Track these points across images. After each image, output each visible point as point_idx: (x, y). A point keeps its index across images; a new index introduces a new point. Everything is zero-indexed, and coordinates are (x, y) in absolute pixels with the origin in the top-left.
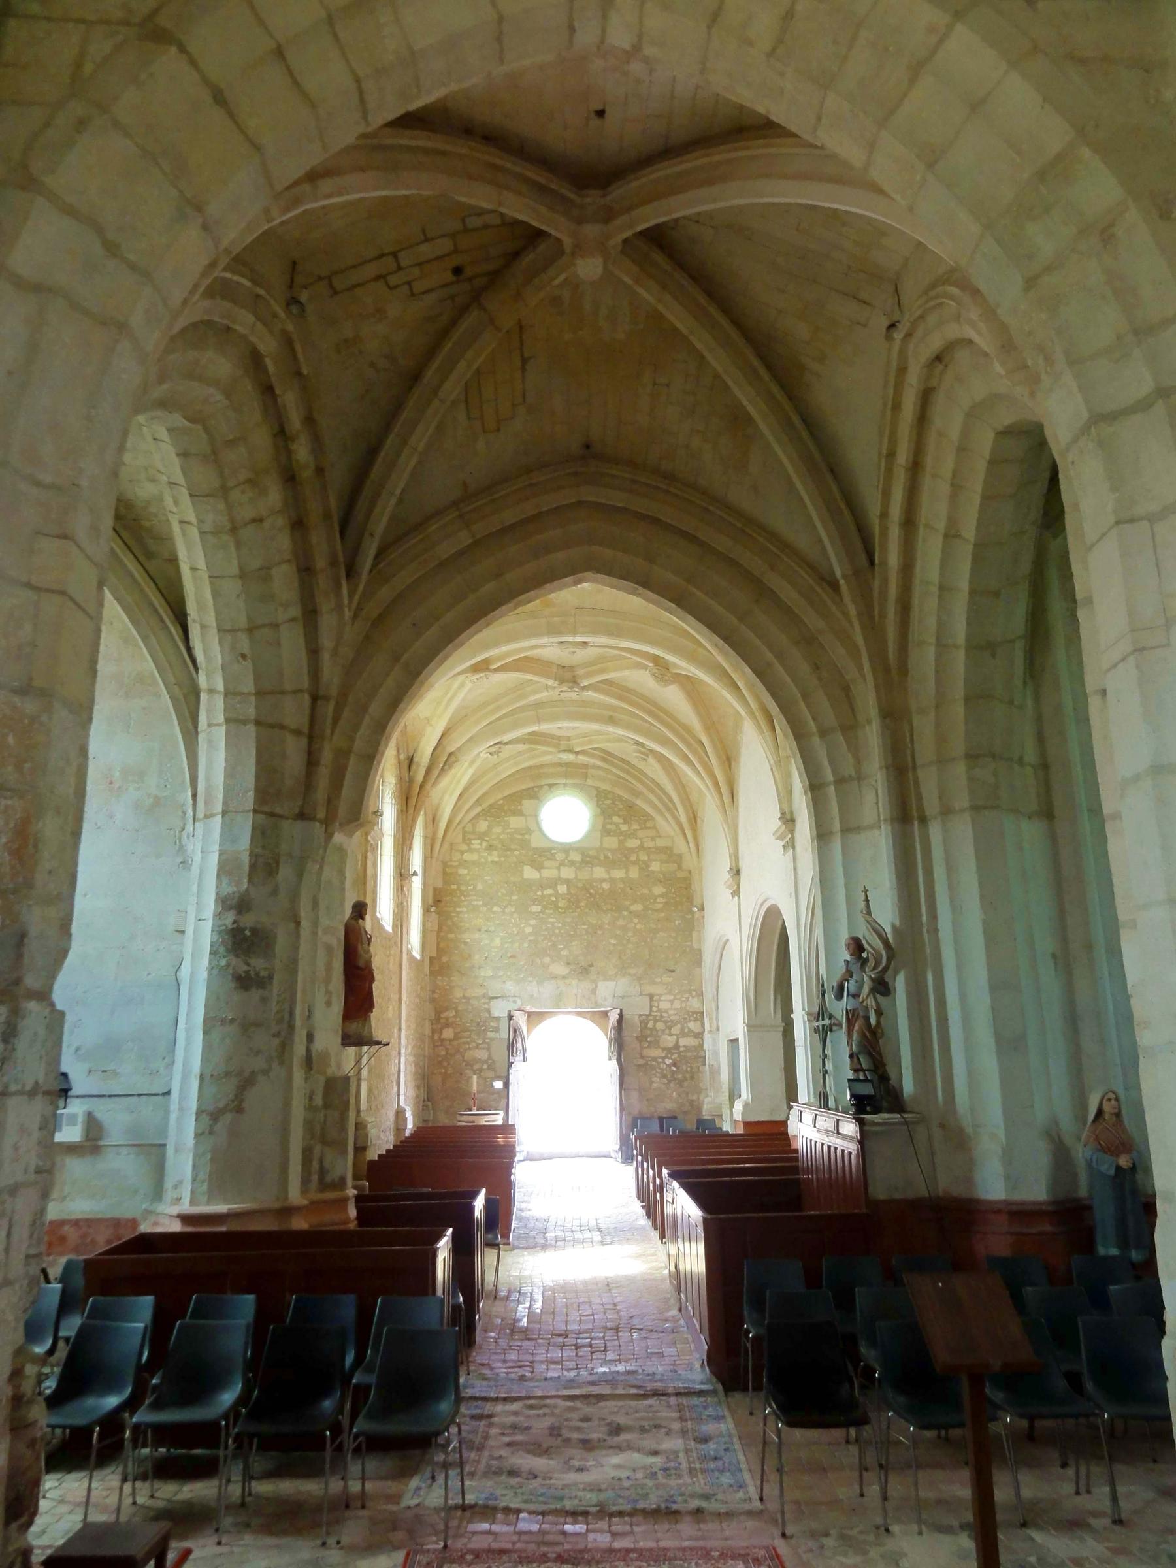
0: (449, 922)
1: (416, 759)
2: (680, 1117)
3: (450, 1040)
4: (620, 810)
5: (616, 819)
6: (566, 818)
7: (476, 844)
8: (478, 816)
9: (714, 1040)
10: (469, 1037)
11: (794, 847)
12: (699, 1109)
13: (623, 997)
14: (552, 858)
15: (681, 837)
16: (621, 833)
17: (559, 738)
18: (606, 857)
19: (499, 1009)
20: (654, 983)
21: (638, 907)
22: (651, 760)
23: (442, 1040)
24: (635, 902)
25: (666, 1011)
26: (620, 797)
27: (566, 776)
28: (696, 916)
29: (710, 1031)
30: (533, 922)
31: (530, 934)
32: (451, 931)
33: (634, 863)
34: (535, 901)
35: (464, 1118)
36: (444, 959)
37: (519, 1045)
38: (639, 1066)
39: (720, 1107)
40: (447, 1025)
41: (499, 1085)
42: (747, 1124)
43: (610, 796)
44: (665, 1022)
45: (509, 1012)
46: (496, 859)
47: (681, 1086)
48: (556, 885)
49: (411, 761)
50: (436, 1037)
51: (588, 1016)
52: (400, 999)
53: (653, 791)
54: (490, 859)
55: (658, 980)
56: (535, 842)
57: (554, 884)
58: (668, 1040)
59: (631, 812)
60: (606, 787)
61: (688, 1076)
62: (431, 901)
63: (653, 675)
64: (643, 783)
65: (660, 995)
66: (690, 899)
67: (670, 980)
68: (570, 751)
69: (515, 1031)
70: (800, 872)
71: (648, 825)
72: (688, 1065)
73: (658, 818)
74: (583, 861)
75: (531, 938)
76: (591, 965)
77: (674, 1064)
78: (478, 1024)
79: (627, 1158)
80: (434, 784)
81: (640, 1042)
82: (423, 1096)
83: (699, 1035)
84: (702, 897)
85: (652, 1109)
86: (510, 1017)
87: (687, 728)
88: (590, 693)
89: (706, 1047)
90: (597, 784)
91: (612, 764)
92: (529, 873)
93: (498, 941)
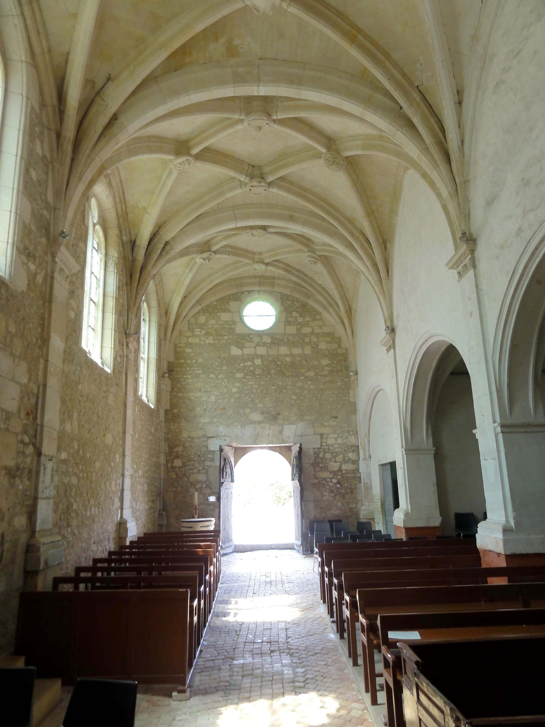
0: (179, 386)
1: (137, 243)
2: (344, 521)
3: (180, 468)
4: (298, 308)
5: (294, 314)
6: (260, 314)
7: (197, 331)
8: (198, 313)
9: (367, 465)
10: (193, 465)
11: (474, 267)
12: (357, 515)
13: (302, 436)
14: (251, 340)
15: (341, 325)
16: (299, 323)
17: (254, 253)
18: (288, 340)
19: (214, 445)
20: (323, 426)
21: (311, 374)
22: (320, 267)
23: (173, 468)
24: (309, 370)
25: (332, 445)
26: (297, 300)
27: (260, 284)
28: (352, 379)
29: (364, 459)
30: (238, 385)
31: (236, 393)
32: (180, 391)
33: (309, 343)
34: (239, 370)
35: (185, 524)
36: (175, 411)
37: (228, 470)
38: (314, 484)
39: (373, 513)
40: (177, 457)
41: (212, 499)
42: (408, 530)
43: (290, 299)
44: (332, 453)
45: (221, 446)
46: (212, 342)
47: (344, 498)
48: (253, 359)
49: (133, 244)
50: (169, 465)
51: (277, 449)
52: (124, 432)
53: (320, 293)
54: (207, 342)
55: (326, 424)
56: (239, 330)
57: (251, 358)
58: (334, 466)
59: (304, 309)
60: (288, 292)
61: (348, 490)
62: (165, 370)
63: (326, 160)
64: (311, 286)
65: (328, 434)
66: (347, 368)
67: (335, 423)
68: (262, 262)
69: (225, 460)
70: (484, 286)
71: (318, 317)
72: (349, 484)
73: (325, 314)
74: (272, 343)
75: (236, 396)
76: (279, 414)
77: (339, 483)
78: (199, 456)
79: (308, 551)
80: (154, 265)
81: (314, 467)
82: (159, 505)
83: (356, 462)
84: (356, 366)
85: (324, 515)
86: (221, 450)
87: (351, 221)
88: (274, 190)
89: (361, 470)
90: (282, 290)
91: (292, 274)
92: (235, 351)
93: (213, 398)
